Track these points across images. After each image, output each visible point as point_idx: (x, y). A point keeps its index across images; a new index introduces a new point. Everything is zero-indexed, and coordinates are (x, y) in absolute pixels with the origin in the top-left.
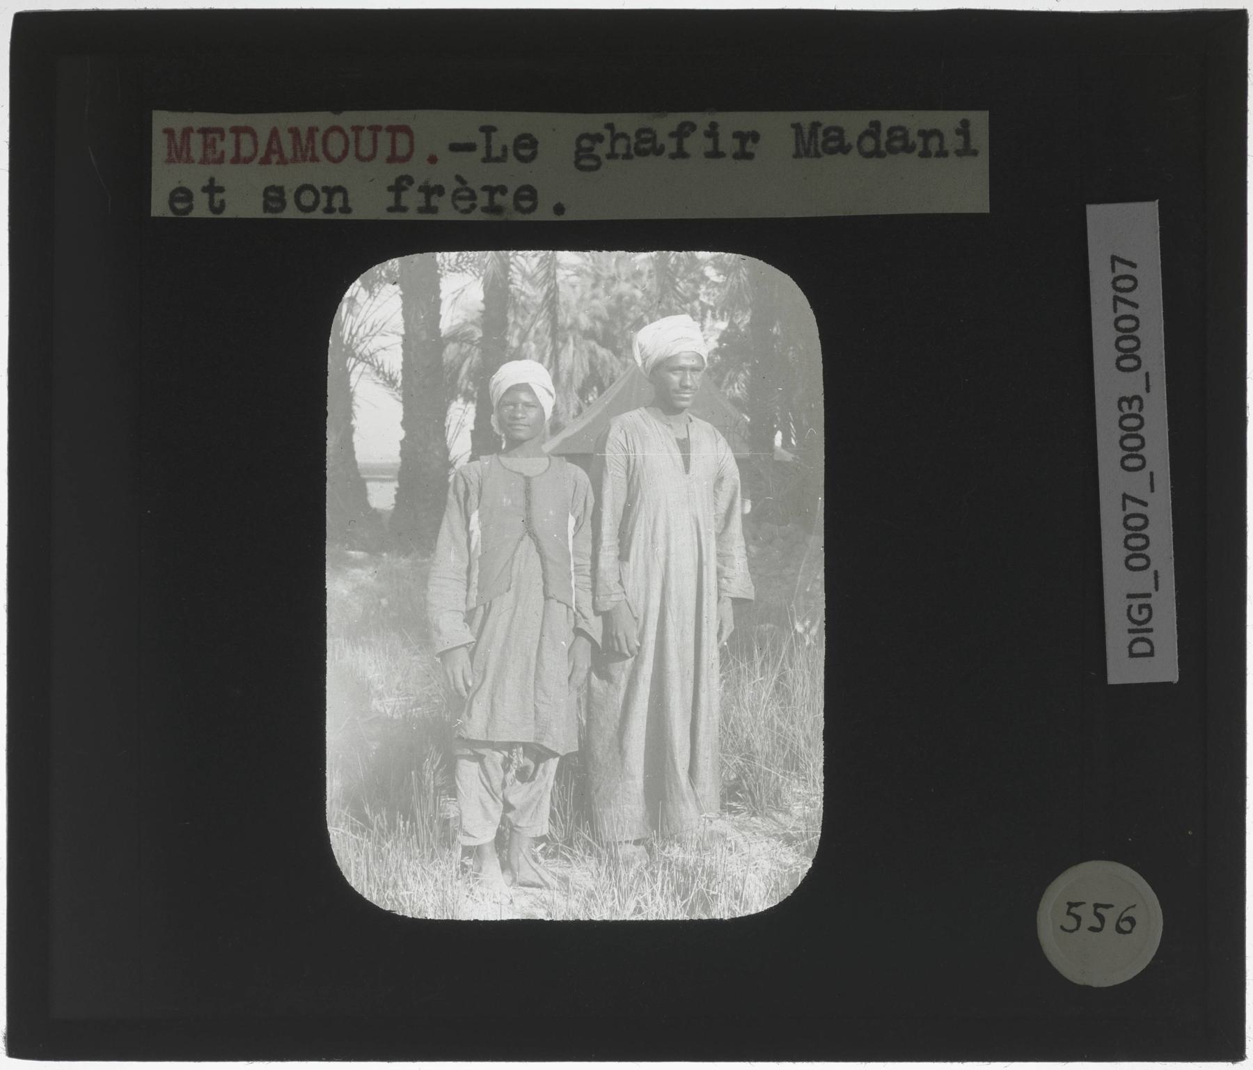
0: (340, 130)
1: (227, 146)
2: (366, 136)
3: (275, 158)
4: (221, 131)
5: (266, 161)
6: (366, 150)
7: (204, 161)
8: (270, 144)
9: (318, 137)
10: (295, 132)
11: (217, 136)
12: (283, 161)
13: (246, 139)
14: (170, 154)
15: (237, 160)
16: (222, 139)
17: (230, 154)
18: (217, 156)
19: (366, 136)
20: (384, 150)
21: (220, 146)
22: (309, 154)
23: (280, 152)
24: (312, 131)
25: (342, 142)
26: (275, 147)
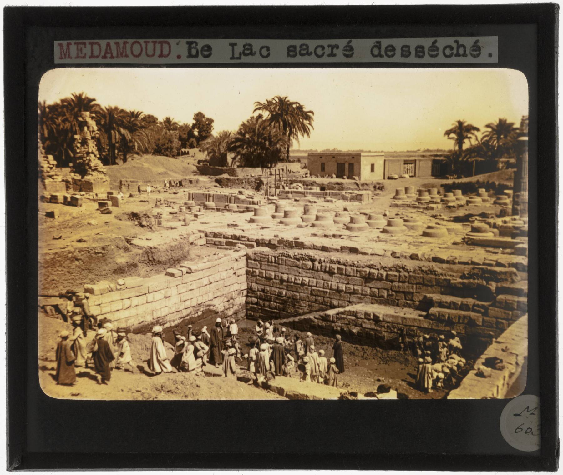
0: (139, 43)
1: (87, 50)
2: (150, 46)
3: (109, 56)
4: (85, 44)
5: (105, 57)
6: (150, 52)
7: (78, 57)
8: (106, 49)
9: (128, 46)
10: (117, 44)
11: (83, 46)
12: (112, 57)
13: (96, 47)
14: (61, 55)
15: (92, 56)
16: (85, 47)
17: (89, 54)
18: (83, 55)
19: (150, 46)
20: (158, 52)
21: (84, 50)
22: (124, 54)
23: (112, 54)
24: (125, 43)
25: (140, 49)
26: (109, 51)
